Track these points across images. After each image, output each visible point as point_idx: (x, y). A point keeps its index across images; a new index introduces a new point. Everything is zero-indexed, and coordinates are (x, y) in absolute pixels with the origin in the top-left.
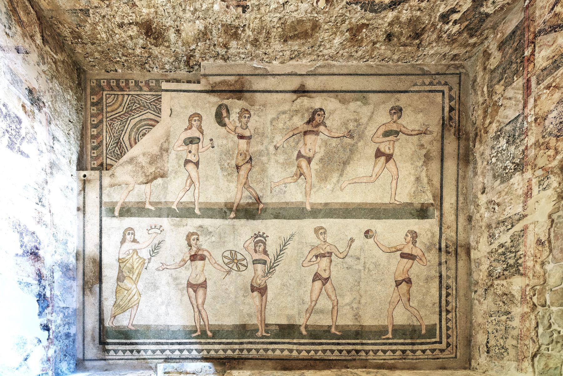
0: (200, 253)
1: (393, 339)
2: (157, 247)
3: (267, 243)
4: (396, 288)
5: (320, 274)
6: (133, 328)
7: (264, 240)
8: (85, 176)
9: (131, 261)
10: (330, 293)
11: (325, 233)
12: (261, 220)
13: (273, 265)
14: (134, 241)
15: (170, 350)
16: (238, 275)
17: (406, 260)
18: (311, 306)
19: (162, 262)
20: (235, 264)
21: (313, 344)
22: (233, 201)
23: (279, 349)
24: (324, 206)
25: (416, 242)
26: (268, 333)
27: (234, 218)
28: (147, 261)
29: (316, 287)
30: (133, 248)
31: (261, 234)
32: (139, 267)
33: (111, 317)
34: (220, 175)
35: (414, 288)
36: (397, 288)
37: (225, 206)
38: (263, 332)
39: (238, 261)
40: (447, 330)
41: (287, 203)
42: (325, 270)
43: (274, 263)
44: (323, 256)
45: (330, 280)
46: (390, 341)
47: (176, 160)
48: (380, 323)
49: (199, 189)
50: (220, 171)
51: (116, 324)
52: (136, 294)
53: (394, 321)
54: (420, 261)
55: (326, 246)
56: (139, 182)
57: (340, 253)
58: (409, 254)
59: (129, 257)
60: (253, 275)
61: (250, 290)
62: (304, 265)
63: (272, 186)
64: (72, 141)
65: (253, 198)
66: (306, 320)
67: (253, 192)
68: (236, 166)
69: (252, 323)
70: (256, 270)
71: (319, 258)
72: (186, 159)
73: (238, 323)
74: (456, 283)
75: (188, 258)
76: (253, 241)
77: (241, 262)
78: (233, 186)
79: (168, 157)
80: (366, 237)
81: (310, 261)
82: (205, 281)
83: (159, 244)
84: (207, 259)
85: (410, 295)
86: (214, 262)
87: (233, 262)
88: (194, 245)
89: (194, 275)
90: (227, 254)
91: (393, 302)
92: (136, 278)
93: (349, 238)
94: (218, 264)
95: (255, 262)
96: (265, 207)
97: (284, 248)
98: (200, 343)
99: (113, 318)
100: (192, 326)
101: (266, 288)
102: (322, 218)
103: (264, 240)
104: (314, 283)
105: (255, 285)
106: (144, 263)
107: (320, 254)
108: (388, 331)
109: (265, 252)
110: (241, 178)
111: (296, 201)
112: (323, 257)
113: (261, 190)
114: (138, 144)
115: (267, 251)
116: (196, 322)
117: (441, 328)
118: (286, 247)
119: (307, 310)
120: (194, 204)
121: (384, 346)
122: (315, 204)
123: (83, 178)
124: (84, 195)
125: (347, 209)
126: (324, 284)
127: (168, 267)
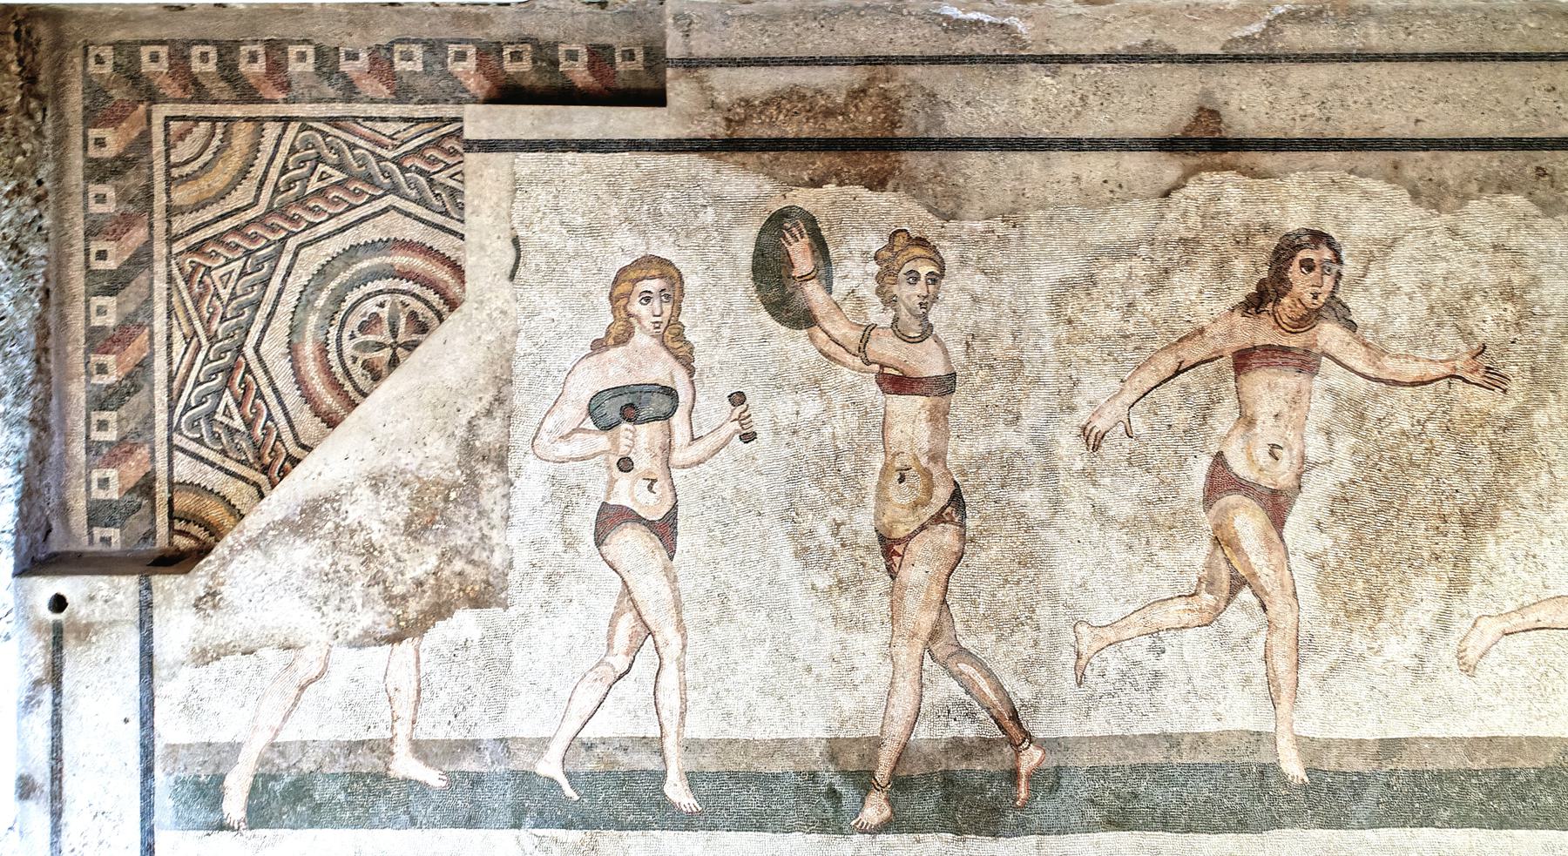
12: (1033, 839)
34: (796, 586)
37: (833, 758)
47: (551, 512)
50: (789, 563)
63: (1083, 649)
65: (983, 715)
67: (983, 684)
78: (868, 646)
96: (1052, 762)
110: (911, 603)
111: (1223, 726)
113: (1026, 670)
125: (1507, 775)
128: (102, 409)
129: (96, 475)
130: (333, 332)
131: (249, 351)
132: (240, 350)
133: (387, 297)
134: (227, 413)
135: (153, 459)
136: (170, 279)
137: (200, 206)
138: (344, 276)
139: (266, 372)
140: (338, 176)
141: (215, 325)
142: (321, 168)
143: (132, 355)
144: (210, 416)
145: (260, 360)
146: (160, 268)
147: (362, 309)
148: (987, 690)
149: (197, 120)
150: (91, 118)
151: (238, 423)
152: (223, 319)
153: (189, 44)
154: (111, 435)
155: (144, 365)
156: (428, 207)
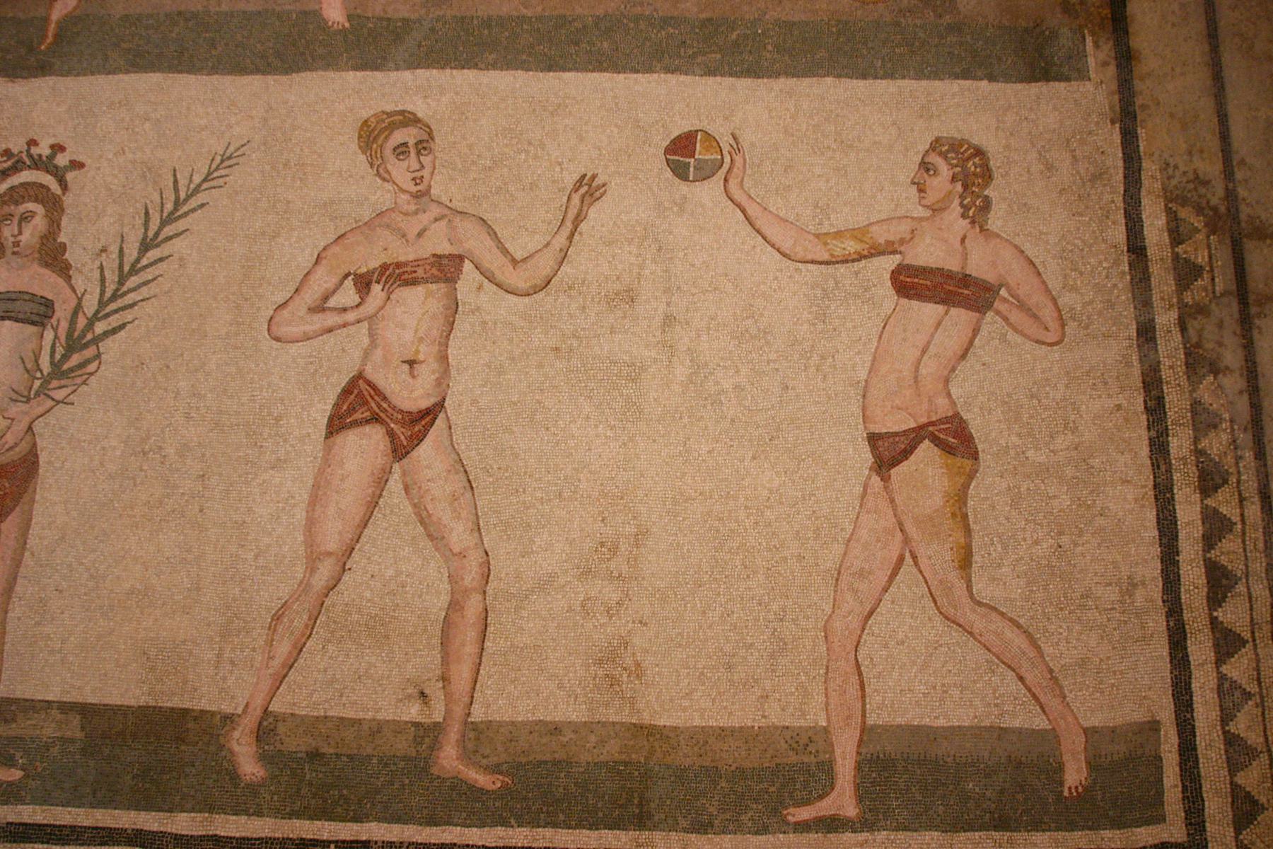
3: (68, 200)
4: (876, 480)
5: (381, 382)
7: (55, 187)
10: (441, 512)
11: (423, 147)
17: (929, 311)
18: (305, 586)
25: (987, 205)
29: (351, 465)
31: (44, 150)
36: (886, 479)
40: (1234, 767)
42: (411, 363)
43: (96, 317)
45: (440, 422)
48: (776, 716)
53: (873, 700)
54: (1015, 316)
55: (425, 218)
57: (515, 262)
58: (949, 275)
66: (265, 685)
71: (376, 288)
74: (1260, 454)
80: (680, 172)
85: (968, 531)
91: (861, 574)
93: (570, 179)
97: (168, 231)
102: (413, 65)
103: (55, 187)
104: (339, 439)
107: (385, 267)
108: (827, 770)
115: (63, 247)
117: (1188, 749)
118: (180, 225)
119: (277, 618)
126: (400, 451)
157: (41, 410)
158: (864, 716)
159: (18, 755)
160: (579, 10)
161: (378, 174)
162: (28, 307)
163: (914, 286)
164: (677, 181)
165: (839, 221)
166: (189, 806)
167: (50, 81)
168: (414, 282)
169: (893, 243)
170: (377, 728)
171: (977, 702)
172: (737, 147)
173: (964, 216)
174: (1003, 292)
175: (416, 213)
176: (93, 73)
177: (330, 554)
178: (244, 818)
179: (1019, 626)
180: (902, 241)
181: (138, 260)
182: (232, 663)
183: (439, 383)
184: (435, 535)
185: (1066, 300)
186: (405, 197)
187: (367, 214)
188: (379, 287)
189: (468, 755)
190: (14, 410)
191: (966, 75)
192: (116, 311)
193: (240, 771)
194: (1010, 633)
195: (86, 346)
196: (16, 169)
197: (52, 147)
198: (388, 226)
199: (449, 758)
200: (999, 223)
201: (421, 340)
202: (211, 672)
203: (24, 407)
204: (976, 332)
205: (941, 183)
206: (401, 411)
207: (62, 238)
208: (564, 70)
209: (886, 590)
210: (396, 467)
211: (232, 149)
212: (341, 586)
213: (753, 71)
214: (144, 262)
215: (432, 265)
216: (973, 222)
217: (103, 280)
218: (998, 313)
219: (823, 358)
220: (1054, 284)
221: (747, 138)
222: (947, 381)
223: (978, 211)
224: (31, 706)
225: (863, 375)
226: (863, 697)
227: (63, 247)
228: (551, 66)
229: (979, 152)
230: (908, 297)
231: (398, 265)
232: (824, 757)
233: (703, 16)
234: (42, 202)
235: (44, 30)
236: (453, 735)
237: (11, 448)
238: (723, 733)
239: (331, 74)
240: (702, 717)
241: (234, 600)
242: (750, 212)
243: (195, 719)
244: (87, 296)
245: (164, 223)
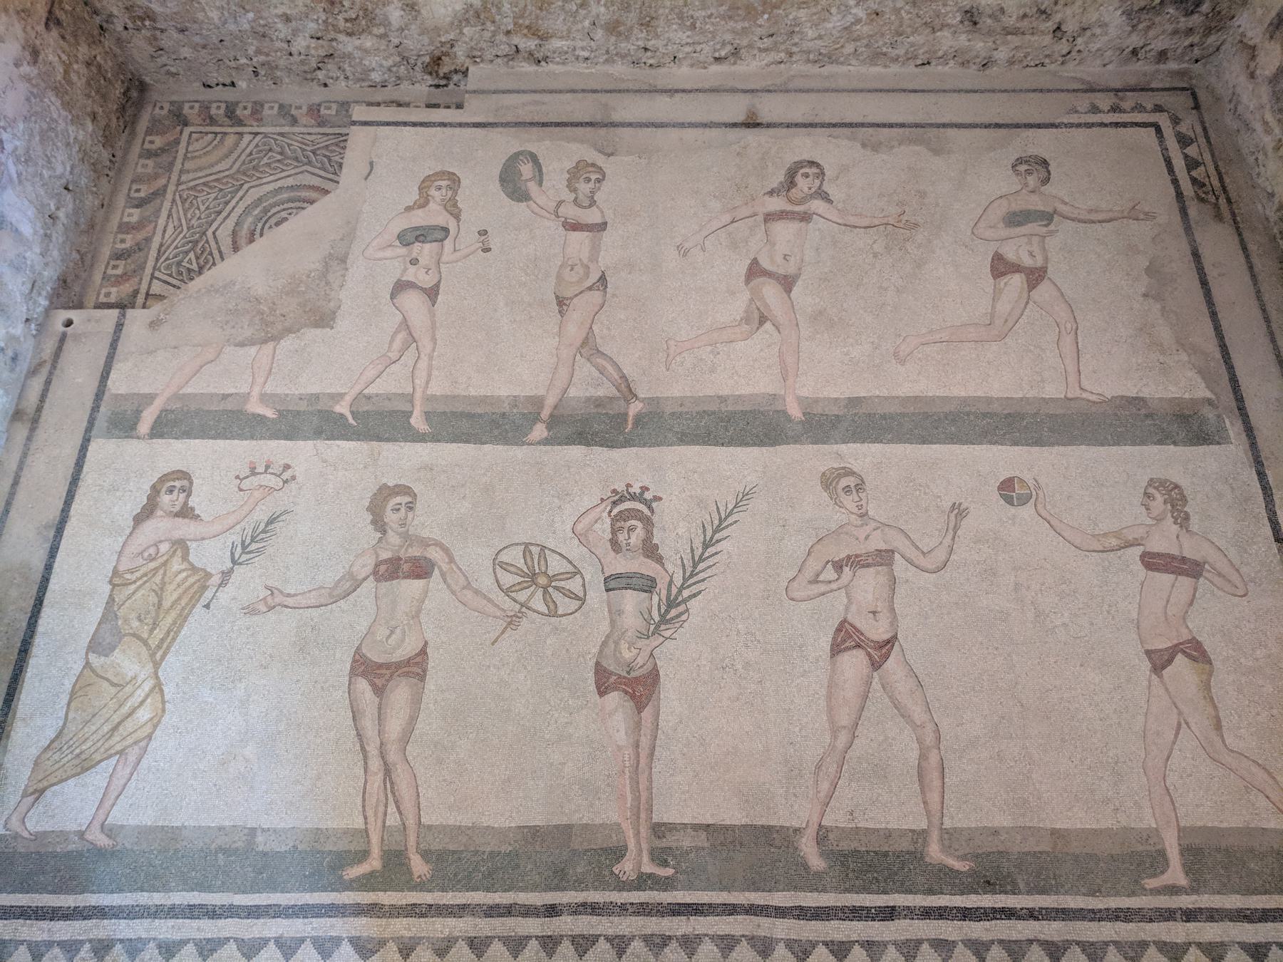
0: (415, 552)
1: (1193, 890)
2: (264, 531)
3: (655, 519)
4: (1154, 676)
5: (858, 625)
6: (103, 841)
7: (646, 511)
8: (69, 323)
9: (158, 579)
11: (860, 487)
13: (680, 591)
14: (186, 512)
15: (240, 943)
16: (547, 629)
17: (1167, 578)
18: (832, 747)
19: (270, 583)
20: (540, 592)
21: (856, 913)
22: (541, 392)
23: (712, 938)
24: (846, 406)
25: (1187, 517)
26: (665, 864)
27: (546, 442)
28: (216, 580)
30: (177, 534)
31: (636, 489)
32: (183, 602)
33: (25, 795)
35: (1224, 679)
36: (1160, 677)
38: (645, 858)
39: (551, 579)
41: (723, 399)
42: (874, 613)
44: (856, 562)
46: (1186, 901)
49: (431, 358)
51: (36, 823)
52: (149, 700)
54: (1217, 580)
55: (868, 529)
56: (240, 339)
57: (923, 553)
58: (1173, 557)
59: (153, 565)
60: (605, 627)
61: (593, 688)
62: (796, 595)
64: (58, 235)
68: (557, 297)
69: (598, 821)
70: (615, 613)
71: (846, 569)
72: (399, 280)
73: (538, 821)
75: (369, 569)
76: (605, 514)
77: (562, 584)
79: (344, 276)
80: (1009, 501)
81: (815, 581)
82: (423, 652)
83: (271, 522)
84: (436, 572)
85: (1215, 707)
86: (462, 581)
87: (534, 582)
88: (395, 526)
89: (382, 633)
90: (514, 556)
92: (162, 640)
93: (947, 505)
94: (477, 592)
95: (614, 583)
97: (717, 536)
98: (373, 910)
99: (31, 799)
100: (353, 833)
101: (653, 677)
103: (646, 511)
104: (839, 658)
105: (611, 668)
106: (204, 588)
107: (849, 557)
108: (1162, 854)
109: (651, 550)
112: (863, 566)
114: (260, 243)
116: (370, 813)
119: (818, 767)
120: (411, 401)
121: (1164, 925)
122: (816, 401)
123: (62, 329)
124: (51, 373)
126: (876, 665)
127: (290, 601)
128: (117, 259)
129: (103, 291)
130: (260, 225)
131: (209, 233)
132: (204, 233)
133: (294, 211)
134: (190, 262)
135: (140, 284)
136: (174, 201)
137: (200, 169)
138: (271, 201)
139: (217, 243)
140: (279, 157)
141: (194, 222)
142: (270, 154)
143: (140, 236)
144: (179, 264)
145: (215, 237)
146: (169, 196)
147: (278, 216)
148: (613, 372)
149: (207, 133)
150: (149, 132)
151: (195, 266)
152: (199, 218)
153: (210, 102)
154: (119, 271)
155: (148, 240)
156: (325, 170)
157: (657, 643)
158: (1177, 821)
159: (669, 859)
160: (934, 410)
161: (836, 503)
162: (640, 582)
163: (1154, 564)
164: (1008, 506)
165: (1104, 527)
166: (781, 887)
167: (634, 449)
168: (868, 566)
169: (1136, 539)
170: (888, 834)
171: (1244, 812)
172: (1038, 487)
173: (1175, 523)
174: (1207, 566)
175: (862, 525)
176: (658, 446)
177: (845, 727)
178: (816, 894)
179: (1259, 765)
180: (1142, 538)
181: (703, 554)
182: (795, 795)
183: (892, 624)
184: (906, 716)
185: (1244, 570)
186: (853, 516)
187: (834, 527)
188: (848, 569)
189: (946, 849)
190: (640, 643)
191: (1160, 442)
192: (694, 584)
193: (810, 864)
194: (1254, 769)
195: (679, 604)
196: (622, 500)
197: (641, 488)
198: (847, 533)
199: (935, 852)
200: (1197, 526)
201: (877, 599)
202: (784, 802)
203: (647, 642)
204: (1195, 590)
205: (1158, 503)
206: (872, 641)
207: (655, 541)
208: (931, 443)
209: (1174, 743)
210: (875, 674)
211: (747, 489)
212: (853, 746)
213: (1039, 442)
214: (706, 555)
215: (877, 555)
216: (1181, 527)
217: (683, 565)
218: (1206, 578)
219: (1110, 606)
220: (1236, 562)
221: (1042, 480)
222: (1184, 619)
223: (1183, 520)
224: (672, 827)
225: (1135, 615)
226: (1175, 809)
227: (657, 546)
228: (924, 441)
229: (1177, 487)
230: (1151, 570)
231: (857, 556)
232: (1159, 847)
233: (1006, 412)
234: (640, 520)
235: (626, 421)
236: (935, 835)
237: (641, 667)
238: (1095, 832)
239: (798, 446)
240: (1081, 823)
241: (791, 757)
242: (1052, 523)
243: (778, 831)
244: (675, 575)
245: (715, 532)
